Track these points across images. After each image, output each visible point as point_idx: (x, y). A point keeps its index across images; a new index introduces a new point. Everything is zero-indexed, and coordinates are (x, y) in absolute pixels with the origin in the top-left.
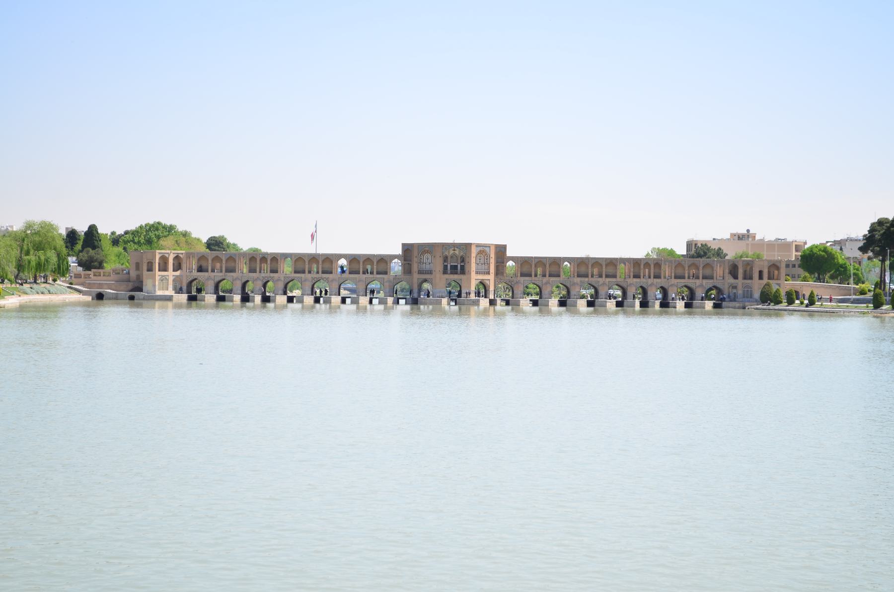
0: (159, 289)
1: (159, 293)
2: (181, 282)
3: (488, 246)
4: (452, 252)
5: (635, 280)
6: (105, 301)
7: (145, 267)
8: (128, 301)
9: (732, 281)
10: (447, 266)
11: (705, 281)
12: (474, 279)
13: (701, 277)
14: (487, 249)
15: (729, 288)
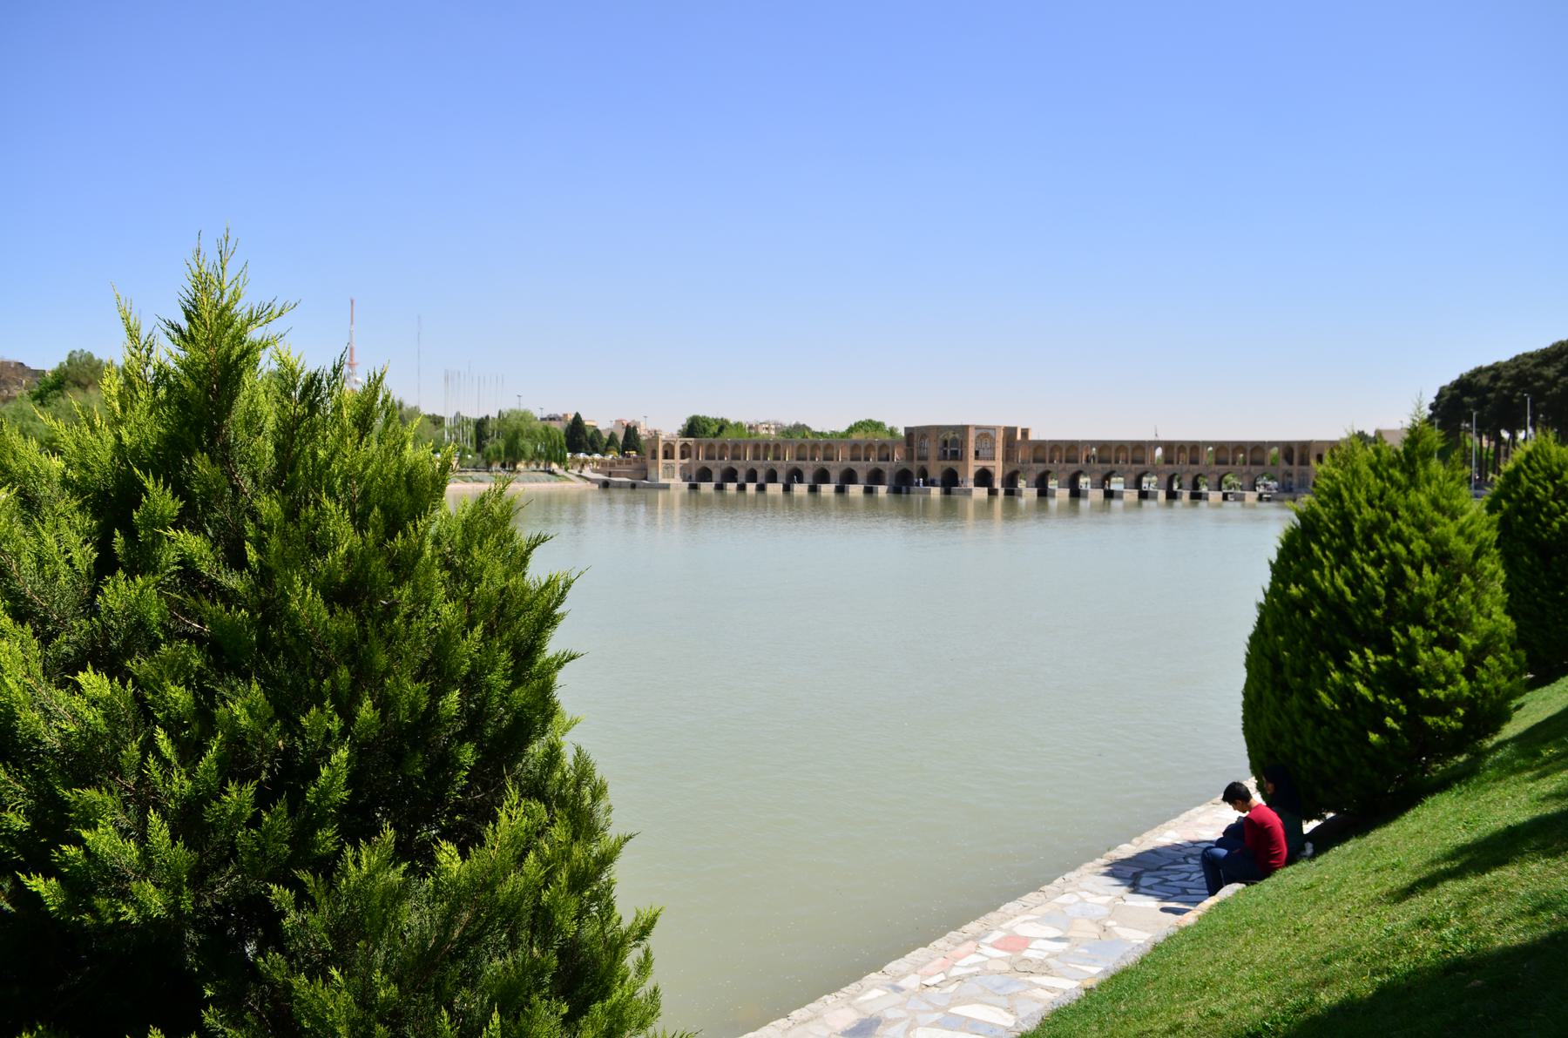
0: (664, 477)
1: (662, 481)
2: (690, 469)
3: (994, 429)
4: (951, 436)
5: (1167, 466)
6: (637, 490)
7: (649, 455)
8: (629, 490)
9: (1286, 467)
10: (945, 452)
11: (1253, 468)
12: (973, 466)
13: (1248, 462)
14: (991, 432)
15: (1284, 475)
